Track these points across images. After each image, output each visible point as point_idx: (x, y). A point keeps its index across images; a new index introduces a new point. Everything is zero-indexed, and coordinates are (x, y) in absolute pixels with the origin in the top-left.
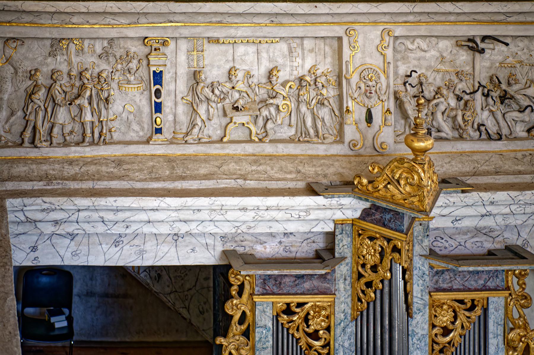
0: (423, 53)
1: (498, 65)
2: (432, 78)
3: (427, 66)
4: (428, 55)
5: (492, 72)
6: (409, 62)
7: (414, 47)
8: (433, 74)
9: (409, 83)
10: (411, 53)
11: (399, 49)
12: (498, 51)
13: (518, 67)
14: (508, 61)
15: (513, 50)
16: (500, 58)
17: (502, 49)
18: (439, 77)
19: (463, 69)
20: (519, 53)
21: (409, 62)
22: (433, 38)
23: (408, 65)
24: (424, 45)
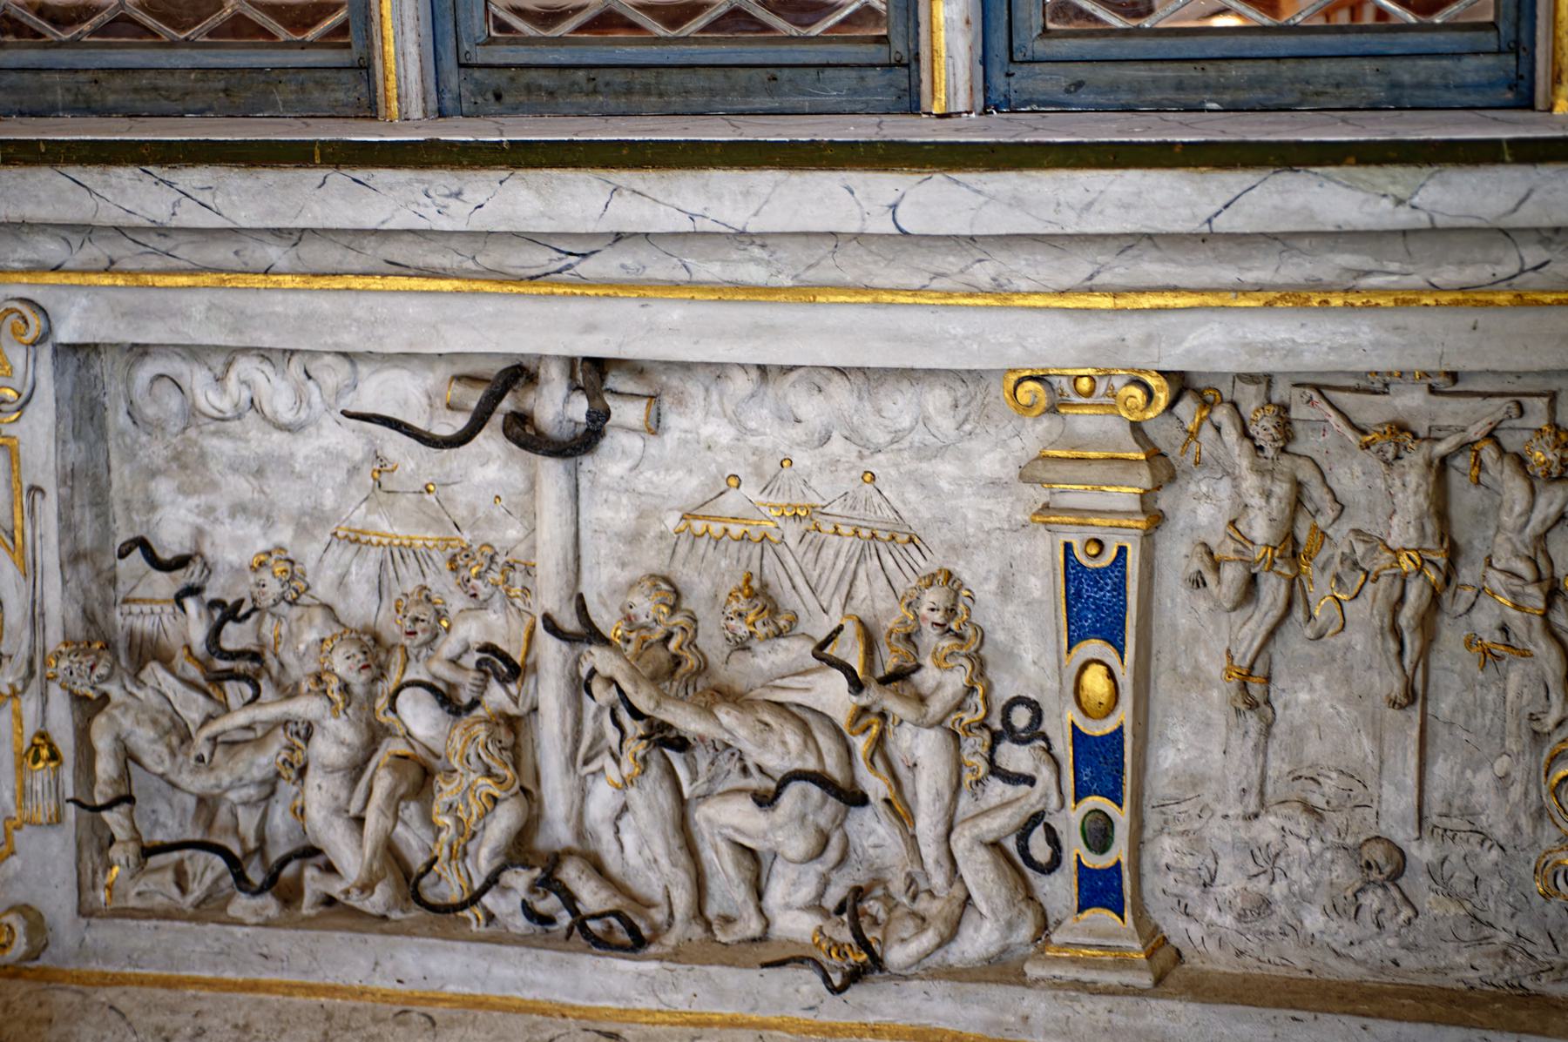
0: (277, 436)
1: (672, 521)
2: (329, 575)
3: (303, 513)
4: (304, 449)
5: (652, 560)
6: (213, 486)
7: (225, 404)
8: (329, 558)
9: (208, 595)
10: (215, 433)
11: (150, 411)
12: (684, 443)
13: (792, 541)
14: (732, 503)
15: (768, 443)
16: (689, 486)
17: (707, 431)
18: (362, 572)
19: (491, 537)
20: (802, 459)
21: (213, 486)
22: (328, 359)
23: (202, 500)
24: (279, 401)
